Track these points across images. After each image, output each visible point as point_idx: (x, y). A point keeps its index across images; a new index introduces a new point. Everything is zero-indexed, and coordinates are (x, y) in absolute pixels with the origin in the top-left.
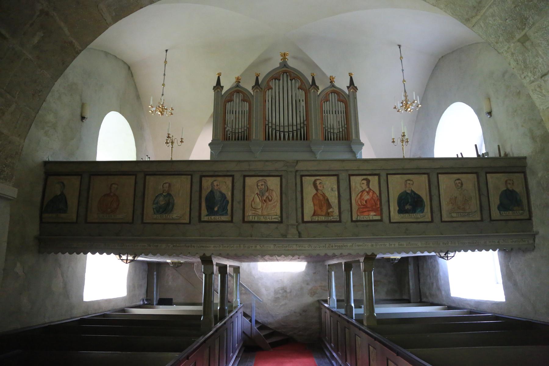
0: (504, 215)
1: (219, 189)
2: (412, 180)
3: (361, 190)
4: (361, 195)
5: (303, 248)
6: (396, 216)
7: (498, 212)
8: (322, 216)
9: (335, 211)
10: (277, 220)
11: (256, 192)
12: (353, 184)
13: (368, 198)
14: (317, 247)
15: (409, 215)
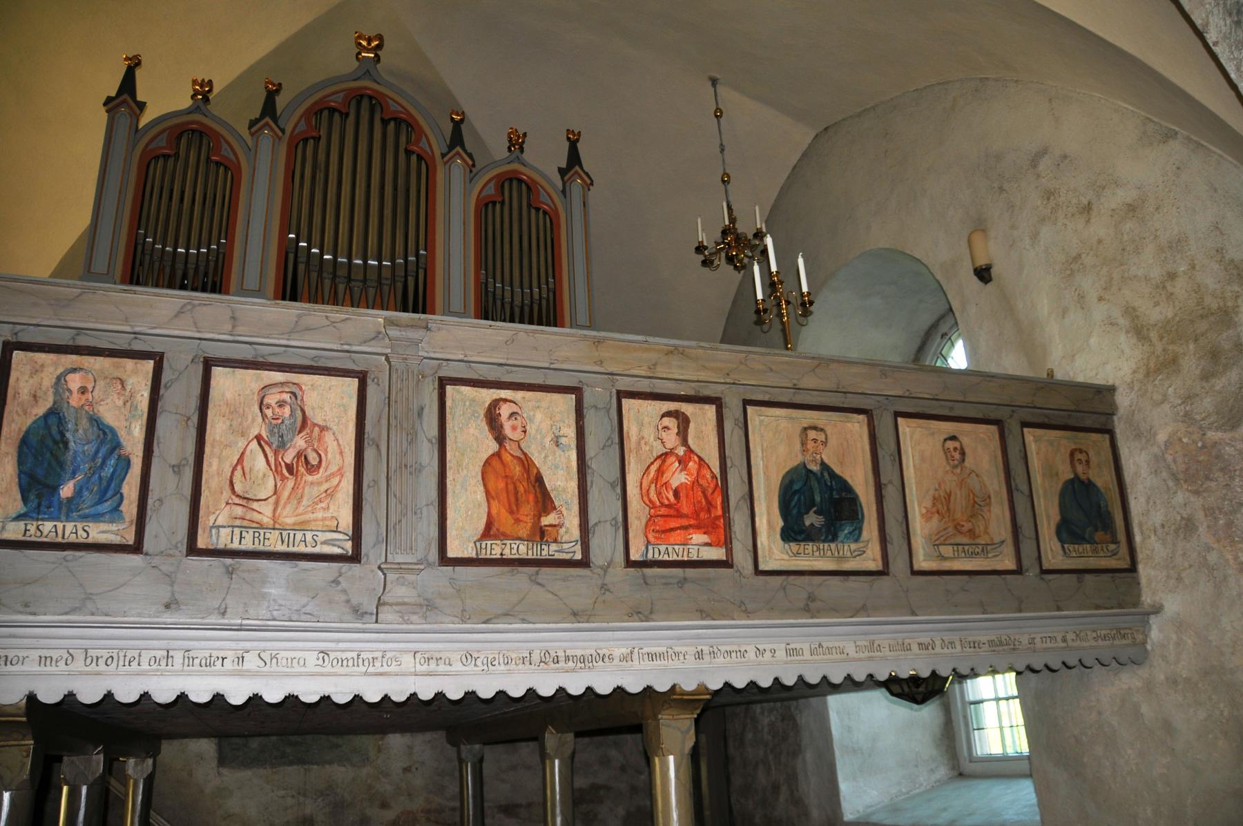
0: (1074, 555)
1: (91, 405)
2: (822, 430)
3: (659, 449)
4: (660, 466)
5: (442, 668)
6: (775, 554)
7: (1059, 545)
8: (518, 542)
9: (567, 524)
10: (337, 551)
11: (256, 433)
12: (631, 428)
13: (683, 480)
14: (496, 663)
15: (815, 548)
